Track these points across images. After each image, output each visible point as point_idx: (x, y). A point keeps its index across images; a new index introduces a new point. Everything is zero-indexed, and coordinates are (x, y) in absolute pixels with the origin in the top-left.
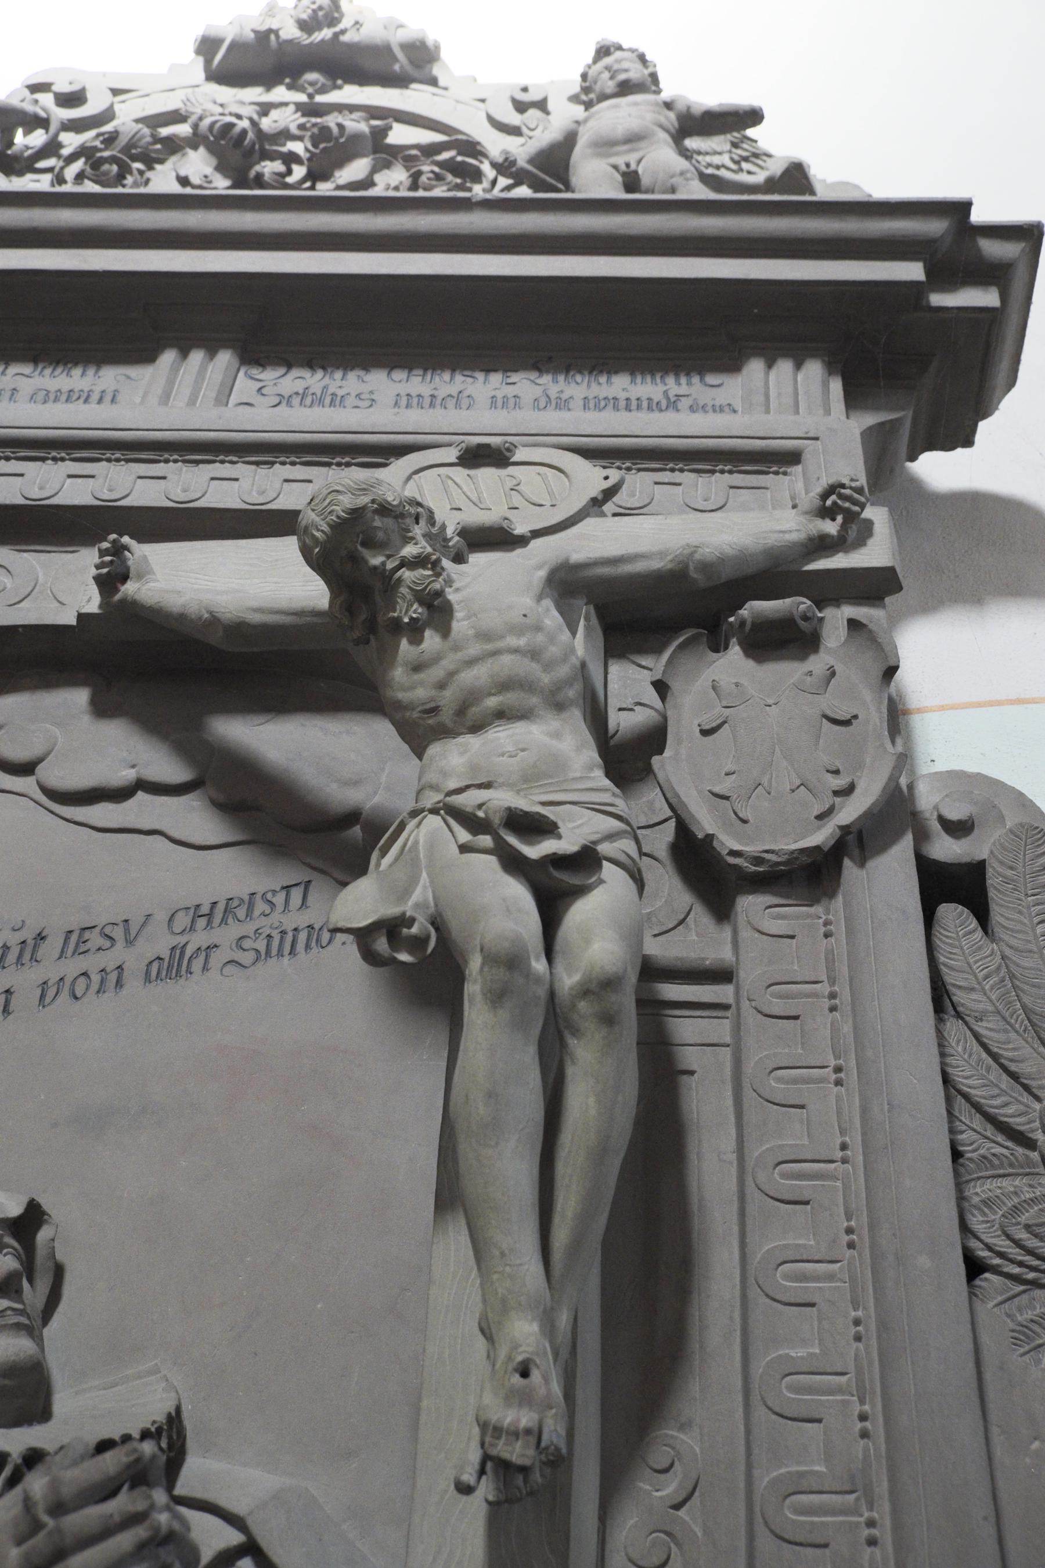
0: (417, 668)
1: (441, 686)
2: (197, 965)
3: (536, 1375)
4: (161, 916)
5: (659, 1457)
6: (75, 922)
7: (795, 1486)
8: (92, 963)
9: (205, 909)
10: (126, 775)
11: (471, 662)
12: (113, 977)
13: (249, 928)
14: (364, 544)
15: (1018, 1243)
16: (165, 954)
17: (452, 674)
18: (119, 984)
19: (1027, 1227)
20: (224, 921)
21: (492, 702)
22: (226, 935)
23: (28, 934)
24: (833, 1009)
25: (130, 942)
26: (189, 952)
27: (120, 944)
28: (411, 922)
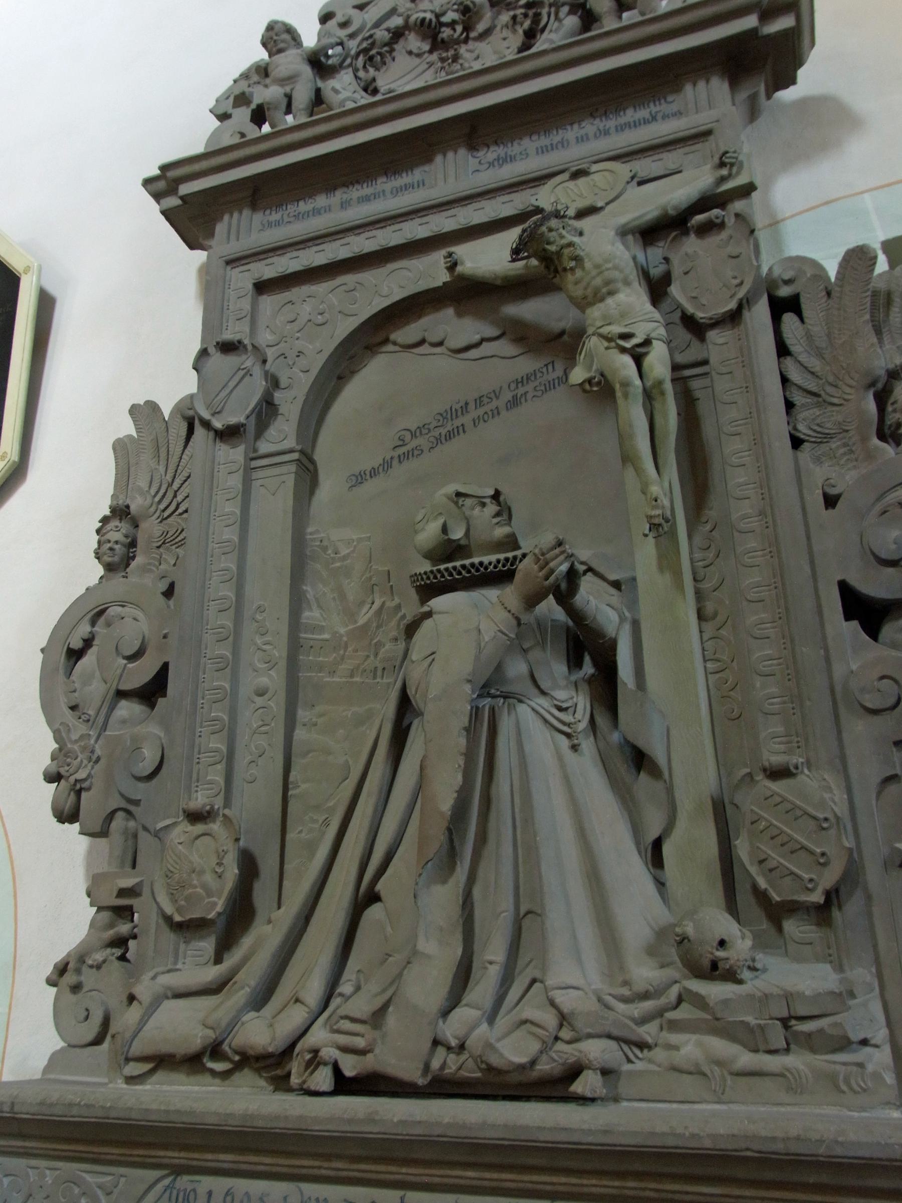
0: (576, 283)
1: (586, 289)
2: (523, 400)
3: (659, 501)
4: (505, 386)
5: (704, 519)
6: (476, 395)
7: (745, 517)
8: (487, 408)
9: (520, 380)
10: (477, 337)
11: (594, 278)
12: (496, 412)
13: (537, 383)
14: (548, 244)
15: (815, 431)
16: (511, 399)
17: (588, 284)
18: (499, 413)
19: (818, 425)
20: (527, 382)
21: (604, 290)
22: (529, 387)
23: (462, 404)
24: (744, 366)
25: (497, 398)
26: (519, 396)
27: (494, 399)
28: (595, 378)
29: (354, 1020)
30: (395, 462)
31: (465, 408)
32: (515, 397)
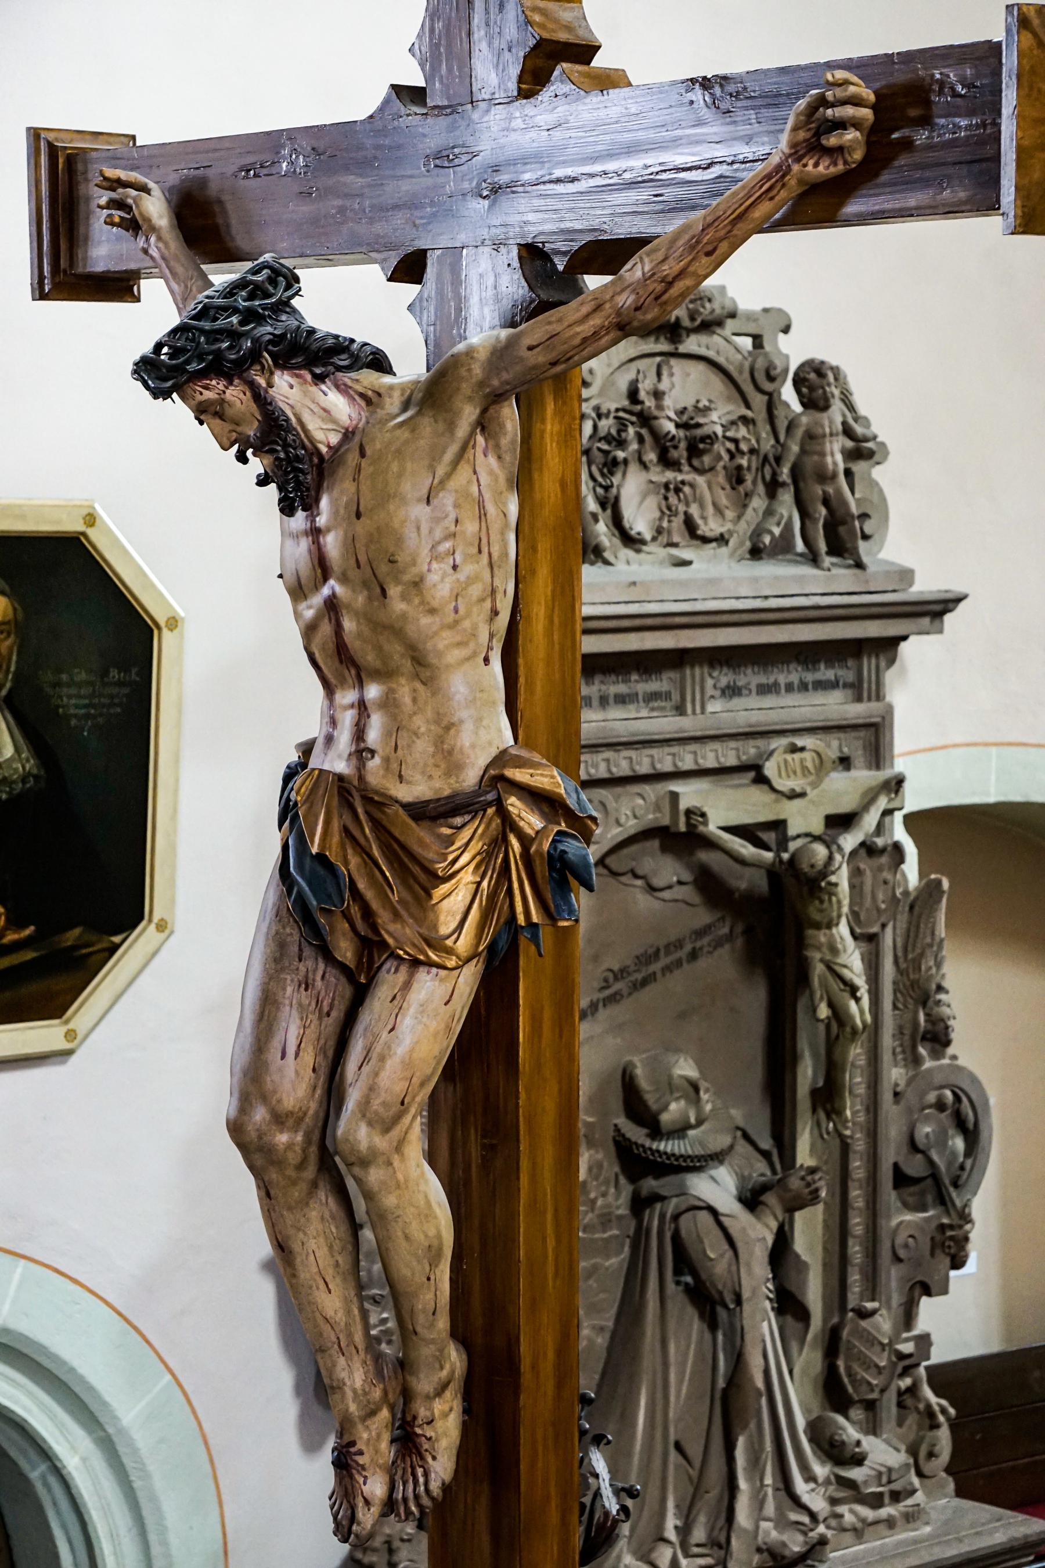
6: (665, 941)
22: (706, 940)
29: (698, 1545)
30: (601, 1004)
31: (657, 953)
32: (694, 949)
